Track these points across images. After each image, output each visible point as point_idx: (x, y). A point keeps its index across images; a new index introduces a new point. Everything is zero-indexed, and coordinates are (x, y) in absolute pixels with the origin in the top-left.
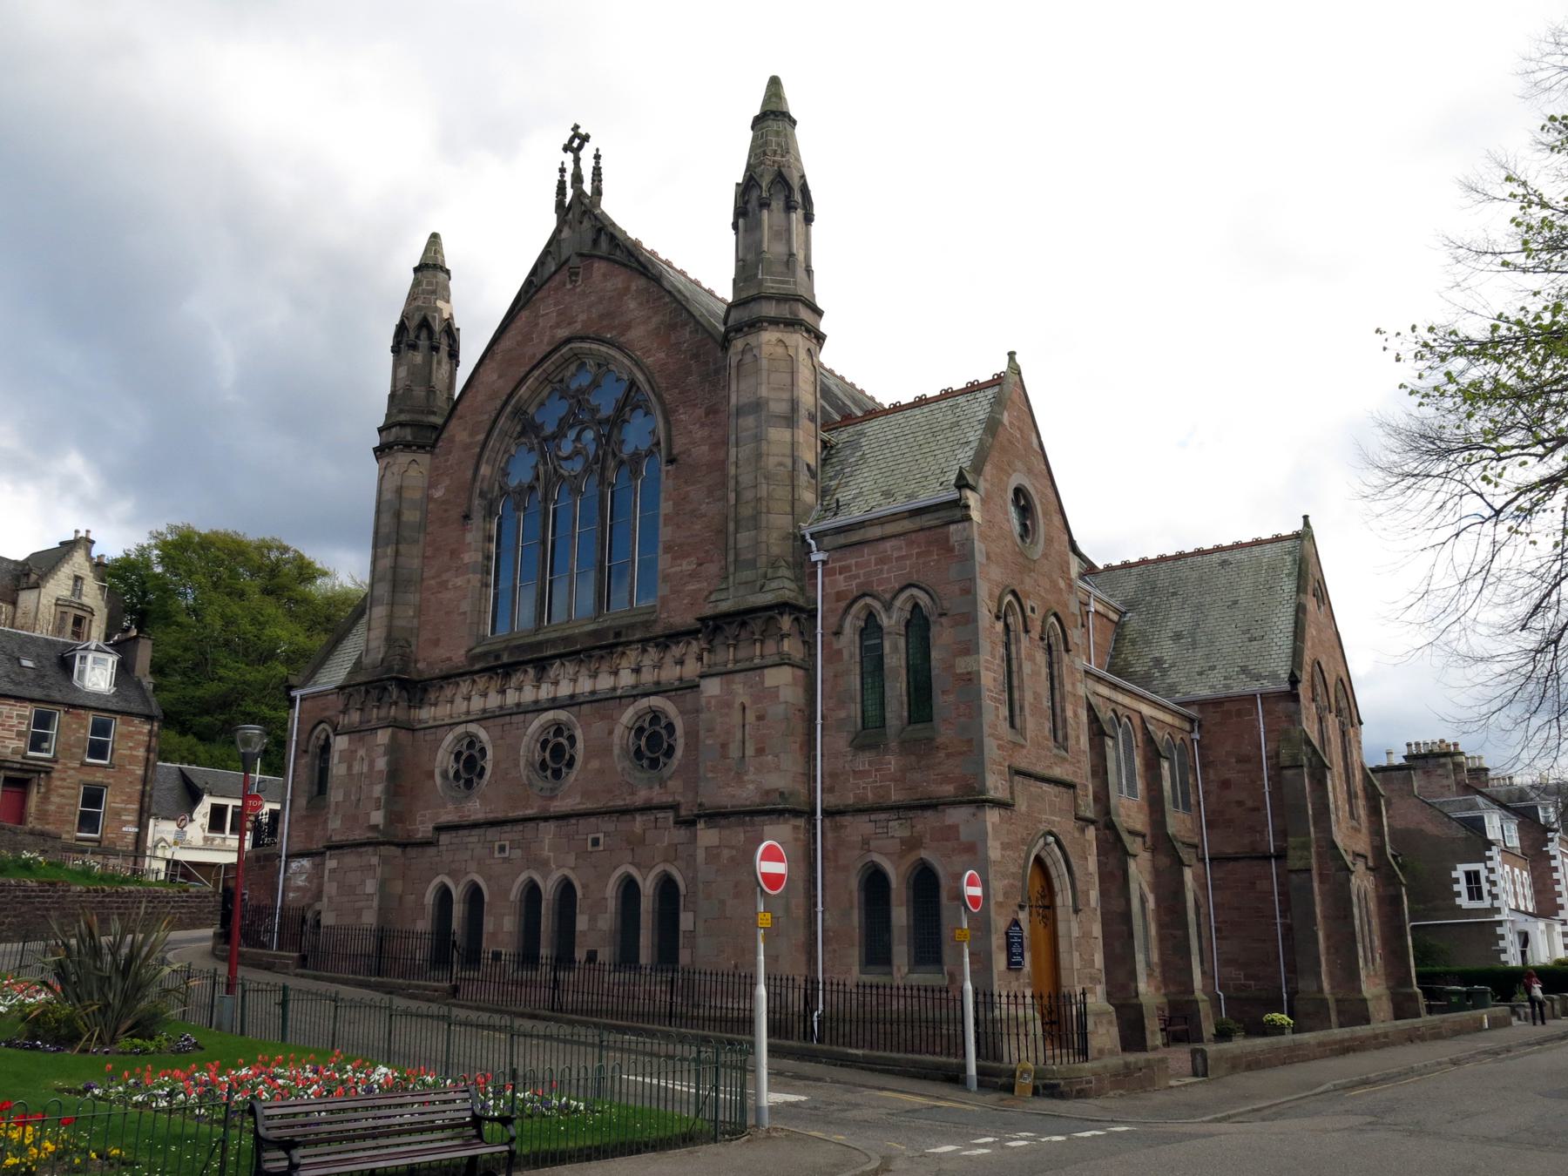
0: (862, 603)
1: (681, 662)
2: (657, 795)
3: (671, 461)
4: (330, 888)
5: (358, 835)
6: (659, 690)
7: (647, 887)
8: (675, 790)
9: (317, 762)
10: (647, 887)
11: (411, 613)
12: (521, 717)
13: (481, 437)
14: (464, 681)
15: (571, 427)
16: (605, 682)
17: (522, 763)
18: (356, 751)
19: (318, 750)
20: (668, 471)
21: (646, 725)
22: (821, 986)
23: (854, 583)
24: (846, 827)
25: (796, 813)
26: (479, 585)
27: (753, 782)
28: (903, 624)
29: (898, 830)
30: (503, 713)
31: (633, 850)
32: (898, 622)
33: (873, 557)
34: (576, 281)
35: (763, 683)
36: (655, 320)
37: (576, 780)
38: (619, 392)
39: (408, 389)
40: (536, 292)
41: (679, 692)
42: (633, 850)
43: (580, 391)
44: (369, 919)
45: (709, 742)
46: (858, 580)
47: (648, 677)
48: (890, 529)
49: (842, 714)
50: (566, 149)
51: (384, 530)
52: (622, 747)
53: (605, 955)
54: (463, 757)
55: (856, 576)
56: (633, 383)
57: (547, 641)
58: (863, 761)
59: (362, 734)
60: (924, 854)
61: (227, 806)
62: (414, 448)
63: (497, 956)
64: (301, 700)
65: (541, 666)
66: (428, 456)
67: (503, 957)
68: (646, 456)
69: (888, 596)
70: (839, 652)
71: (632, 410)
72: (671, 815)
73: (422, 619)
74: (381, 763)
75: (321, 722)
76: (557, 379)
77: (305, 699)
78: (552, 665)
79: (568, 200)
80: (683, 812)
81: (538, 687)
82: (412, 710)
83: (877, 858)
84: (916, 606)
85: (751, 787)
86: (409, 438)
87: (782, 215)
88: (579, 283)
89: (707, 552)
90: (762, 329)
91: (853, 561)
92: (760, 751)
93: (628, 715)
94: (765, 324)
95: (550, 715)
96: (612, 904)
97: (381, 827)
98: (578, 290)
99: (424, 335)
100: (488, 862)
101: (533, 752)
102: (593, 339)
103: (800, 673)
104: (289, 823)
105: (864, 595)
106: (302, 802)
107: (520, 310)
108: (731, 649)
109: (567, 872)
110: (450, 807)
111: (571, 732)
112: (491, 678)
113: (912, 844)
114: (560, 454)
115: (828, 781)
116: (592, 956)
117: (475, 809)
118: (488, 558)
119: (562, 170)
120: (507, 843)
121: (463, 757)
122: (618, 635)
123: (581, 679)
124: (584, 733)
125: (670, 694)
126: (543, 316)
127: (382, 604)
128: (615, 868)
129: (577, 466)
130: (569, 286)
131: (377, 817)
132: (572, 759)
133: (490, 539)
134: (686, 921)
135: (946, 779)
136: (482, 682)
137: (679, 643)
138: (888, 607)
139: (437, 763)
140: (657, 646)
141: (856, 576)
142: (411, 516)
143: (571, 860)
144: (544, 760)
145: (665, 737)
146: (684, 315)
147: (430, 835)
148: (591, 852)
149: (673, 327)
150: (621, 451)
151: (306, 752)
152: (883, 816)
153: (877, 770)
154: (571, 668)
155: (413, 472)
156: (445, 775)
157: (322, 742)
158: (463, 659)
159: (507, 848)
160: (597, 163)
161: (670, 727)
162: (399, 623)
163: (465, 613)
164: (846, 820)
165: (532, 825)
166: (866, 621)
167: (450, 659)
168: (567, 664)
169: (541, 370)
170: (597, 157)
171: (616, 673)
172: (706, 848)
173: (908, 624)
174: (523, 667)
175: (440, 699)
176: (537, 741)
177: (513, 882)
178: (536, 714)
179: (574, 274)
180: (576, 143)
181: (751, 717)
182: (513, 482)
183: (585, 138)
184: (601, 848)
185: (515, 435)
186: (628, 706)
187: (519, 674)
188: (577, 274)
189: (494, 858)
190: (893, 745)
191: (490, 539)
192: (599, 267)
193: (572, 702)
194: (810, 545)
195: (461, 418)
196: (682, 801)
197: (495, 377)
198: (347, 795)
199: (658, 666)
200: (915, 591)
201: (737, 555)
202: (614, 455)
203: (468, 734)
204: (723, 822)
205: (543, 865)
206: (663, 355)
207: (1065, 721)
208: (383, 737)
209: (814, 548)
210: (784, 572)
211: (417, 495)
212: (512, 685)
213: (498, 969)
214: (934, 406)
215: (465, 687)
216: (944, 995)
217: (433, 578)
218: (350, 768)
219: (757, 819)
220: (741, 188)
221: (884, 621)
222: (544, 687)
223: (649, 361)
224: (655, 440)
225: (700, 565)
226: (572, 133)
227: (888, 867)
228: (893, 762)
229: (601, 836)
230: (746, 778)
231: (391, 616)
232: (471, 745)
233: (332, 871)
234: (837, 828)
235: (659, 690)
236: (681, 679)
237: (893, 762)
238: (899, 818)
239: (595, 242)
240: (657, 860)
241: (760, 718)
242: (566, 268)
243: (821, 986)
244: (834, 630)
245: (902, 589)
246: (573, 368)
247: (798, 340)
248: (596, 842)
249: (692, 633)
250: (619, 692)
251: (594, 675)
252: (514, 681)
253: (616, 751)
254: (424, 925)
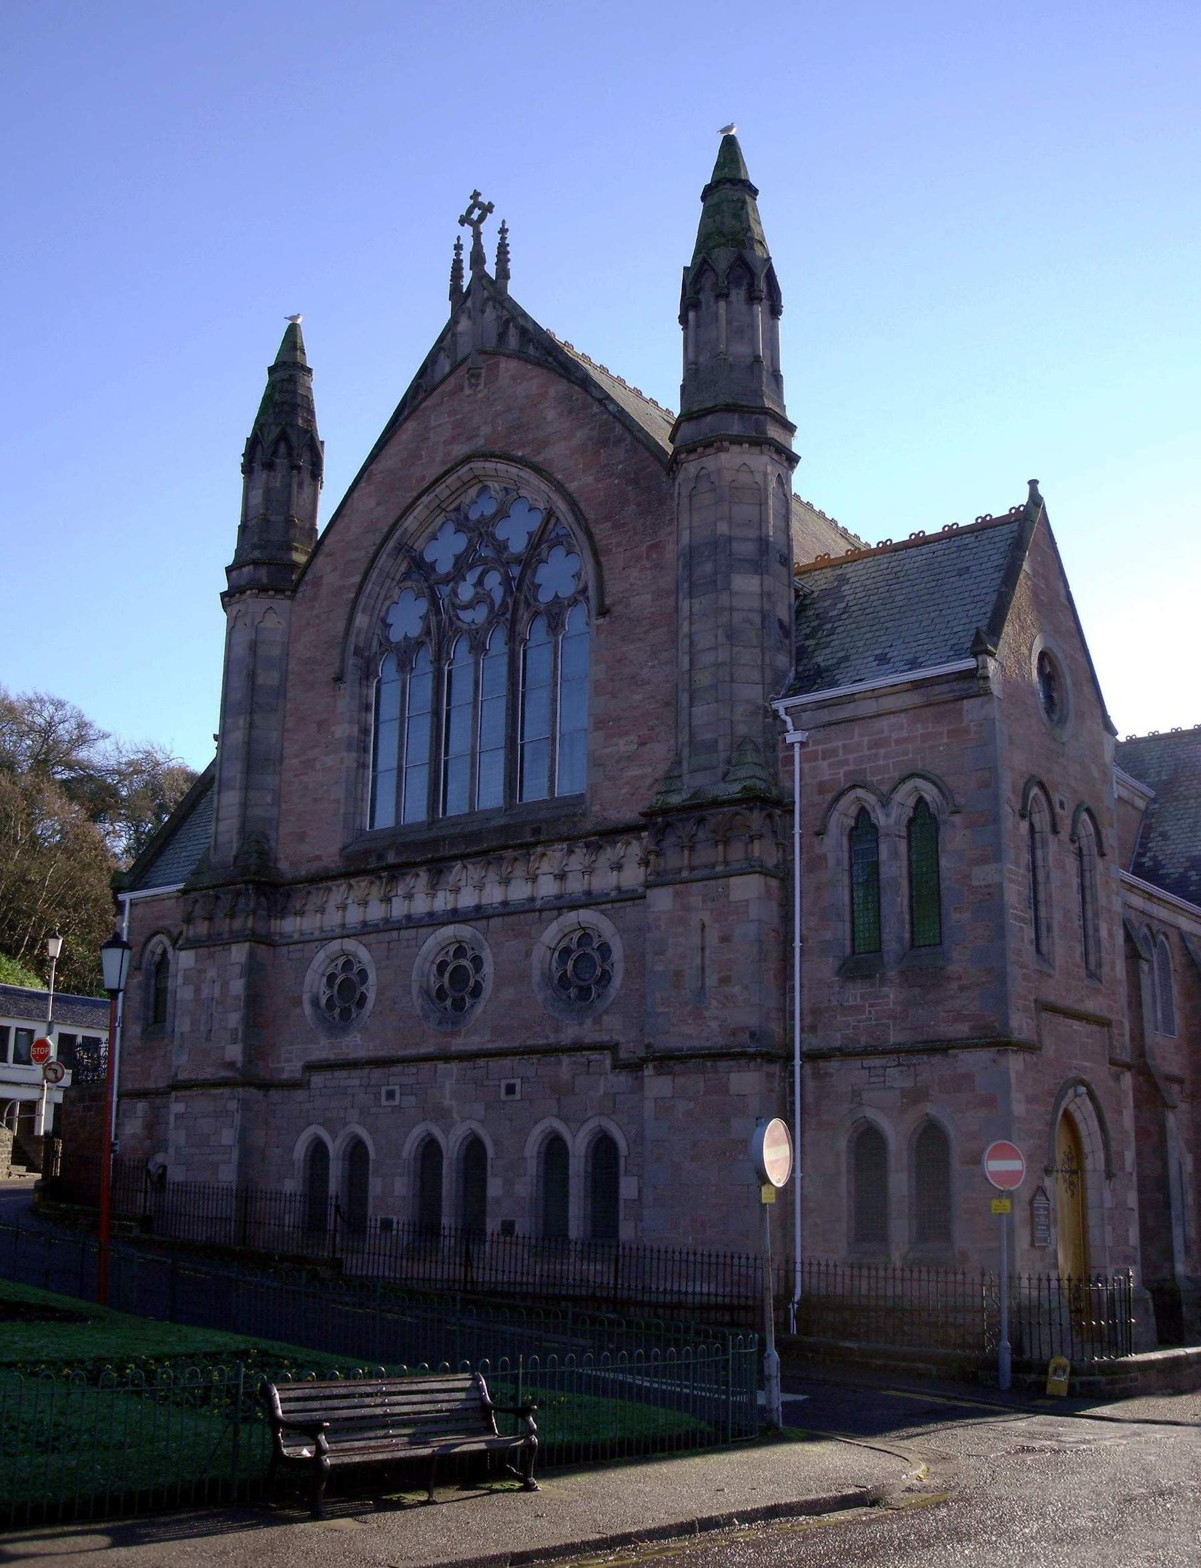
0: (852, 795)
1: (618, 867)
2: (588, 1032)
3: (603, 612)
4: (177, 1137)
5: (208, 1073)
6: (590, 900)
7: (578, 1145)
8: (613, 1027)
9: (153, 982)
10: (578, 1145)
11: (269, 800)
12: (411, 933)
13: (357, 579)
14: (338, 886)
15: (471, 567)
16: (519, 891)
17: (415, 989)
18: (205, 971)
19: (153, 968)
20: (598, 627)
21: (574, 946)
22: (798, 1267)
23: (842, 771)
24: (831, 1075)
25: (769, 1058)
26: (355, 765)
27: (716, 1018)
28: (904, 822)
29: (899, 1079)
30: (388, 925)
31: (558, 1100)
32: (897, 823)
33: (866, 739)
34: (477, 385)
35: (727, 896)
36: (580, 436)
37: (484, 1012)
38: (535, 522)
39: (265, 520)
40: (424, 399)
41: (617, 905)
42: (558, 1100)
43: (483, 520)
44: (227, 1175)
45: (659, 968)
46: (846, 768)
47: (575, 886)
48: (889, 703)
49: (828, 936)
50: (462, 221)
51: (237, 696)
52: (543, 974)
53: (524, 1226)
54: (338, 981)
55: (846, 762)
56: (550, 513)
57: (444, 838)
58: (855, 993)
60: (930, 1108)
61: (8, 1028)
62: (271, 593)
63: (387, 1225)
64: (131, 905)
65: (438, 868)
66: (288, 602)
67: (395, 1226)
68: (570, 606)
69: (885, 788)
70: (823, 858)
71: (551, 548)
73: (283, 807)
74: (238, 986)
75: (156, 933)
76: (452, 507)
77: (136, 904)
78: (450, 869)
79: (465, 283)
80: (623, 1055)
81: (434, 896)
82: (273, 921)
83: (871, 1113)
84: (921, 801)
85: (714, 1025)
86: (265, 580)
87: (744, 308)
88: (481, 387)
89: (652, 729)
90: (721, 449)
91: (840, 744)
92: (725, 981)
93: (551, 934)
94: (726, 444)
95: (448, 931)
96: (532, 1166)
97: (239, 1065)
98: (480, 396)
99: (282, 449)
100: (374, 1110)
101: (428, 976)
102: (500, 457)
103: (774, 883)
104: (120, 1056)
105: (854, 787)
106: (136, 1029)
107: (406, 419)
108: (686, 852)
109: (475, 1125)
110: (324, 1041)
111: (477, 953)
112: (372, 883)
113: (916, 1096)
114: (457, 602)
115: (808, 1020)
116: (508, 1228)
117: (355, 1044)
118: (365, 731)
119: (458, 247)
120: (397, 1088)
121: (338, 981)
122: (536, 831)
123: (488, 888)
124: (494, 955)
125: (603, 906)
126: (434, 428)
127: (234, 788)
128: (536, 1123)
129: (480, 615)
130: (467, 391)
131: (234, 1052)
132: (478, 985)
133: (367, 708)
134: (628, 1187)
135: (958, 1018)
136: (361, 885)
137: (616, 843)
138: (885, 802)
139: (306, 987)
140: (587, 846)
141: (846, 762)
142: (270, 678)
143: (479, 1109)
144: (442, 987)
145: (598, 962)
146: (618, 428)
147: (298, 1075)
148: (505, 1102)
149: (603, 442)
150: (536, 600)
151: (138, 968)
152: (877, 1062)
153: (871, 1006)
154: (474, 872)
155: (271, 622)
156: (315, 1002)
157: (157, 958)
158: (336, 858)
159: (397, 1096)
160: (503, 239)
161: (605, 950)
162: (258, 812)
163: (338, 801)
164: (833, 1066)
165: (427, 1066)
166: (857, 819)
167: (319, 858)
168: (470, 867)
169: (432, 495)
170: (503, 231)
171: (534, 879)
172: (656, 1099)
173: (911, 822)
174: (413, 870)
175: (307, 908)
176: (433, 962)
177: (406, 1136)
178: (431, 929)
179: (474, 375)
180: (476, 215)
181: (712, 937)
182: (396, 636)
183: (488, 208)
184: (518, 1096)
185: (398, 577)
186: (551, 921)
187: (408, 878)
188: (478, 376)
189: (380, 1106)
190: (892, 974)
191: (367, 708)
192: (508, 367)
193: (478, 914)
194: (785, 722)
195: (328, 555)
196: (622, 1039)
197: (373, 503)
199: (589, 871)
200: (919, 782)
201: (692, 736)
202: (529, 605)
203: (344, 953)
204: (678, 1068)
205: (442, 1115)
206: (590, 479)
207: (1098, 942)
208: (239, 953)
209: (790, 726)
210: (750, 757)
211: (276, 652)
212: (400, 892)
213: (389, 1241)
214: (935, 546)
215: (338, 893)
216: (951, 1278)
217: (296, 756)
218: (198, 990)
219: (723, 1064)
220: (692, 274)
221: (881, 819)
222: (441, 895)
223: (572, 486)
224: (581, 586)
225: (642, 744)
226: (472, 202)
227: (886, 1125)
228: (892, 994)
229: (518, 1082)
230: (707, 1014)
231: (245, 805)
232: (348, 965)
233: (178, 1117)
234: (818, 1076)
235: (590, 900)
236: (618, 888)
237: (892, 994)
238: (899, 1065)
239: (502, 336)
240: (589, 1114)
241: (725, 939)
242: (463, 369)
243: (798, 1267)
244: (816, 829)
245: (903, 780)
246: (473, 492)
247: (763, 462)
248: (511, 1089)
249: (631, 830)
250: (539, 903)
251: (506, 882)
252: (401, 889)
253: (536, 978)
254: (292, 1185)
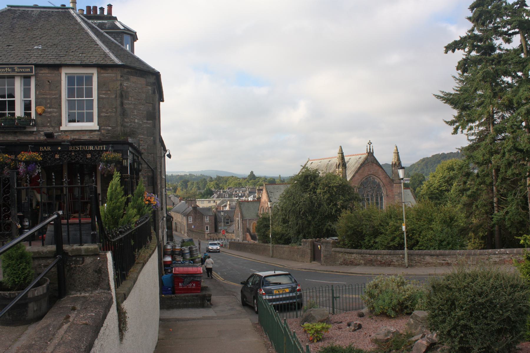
36: (384, 176)
149: (386, 177)
183: (371, 143)
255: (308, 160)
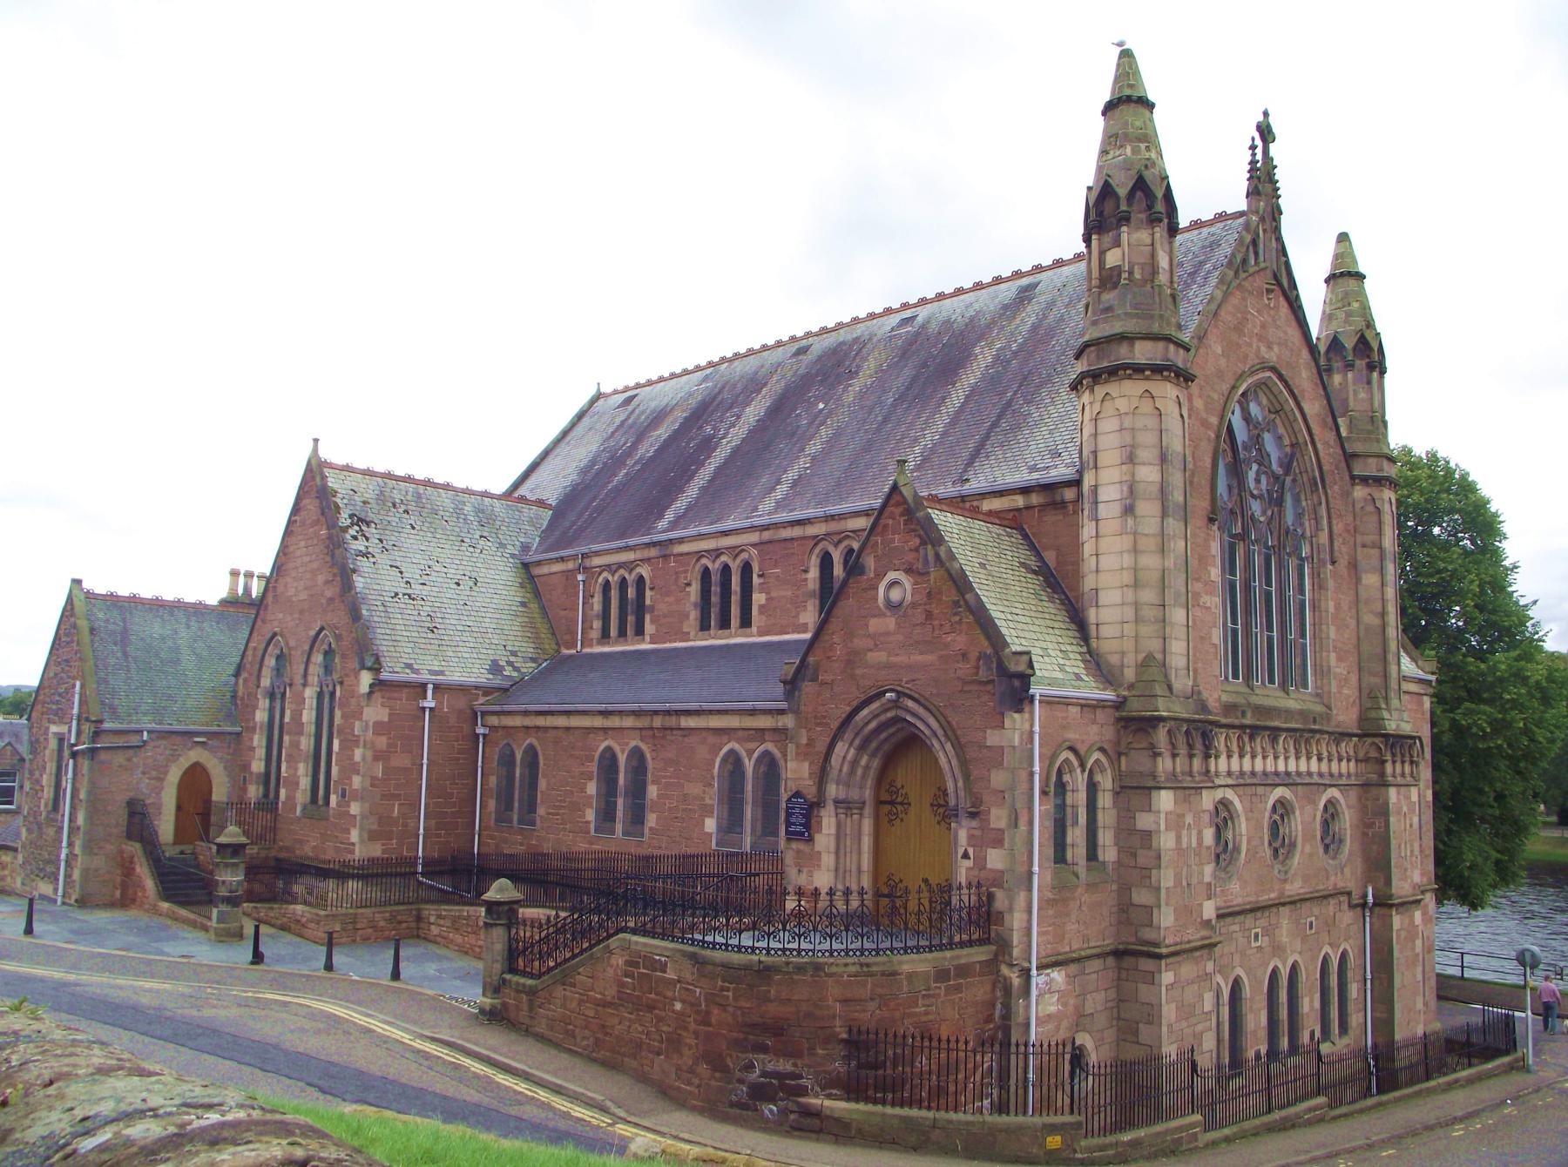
59: (1187, 792)
62: (1148, 373)
72: (1344, 899)
119: (1253, 147)
165: (1274, 910)
198: (1178, 876)
233: (1170, 987)
255: (592, 392)
